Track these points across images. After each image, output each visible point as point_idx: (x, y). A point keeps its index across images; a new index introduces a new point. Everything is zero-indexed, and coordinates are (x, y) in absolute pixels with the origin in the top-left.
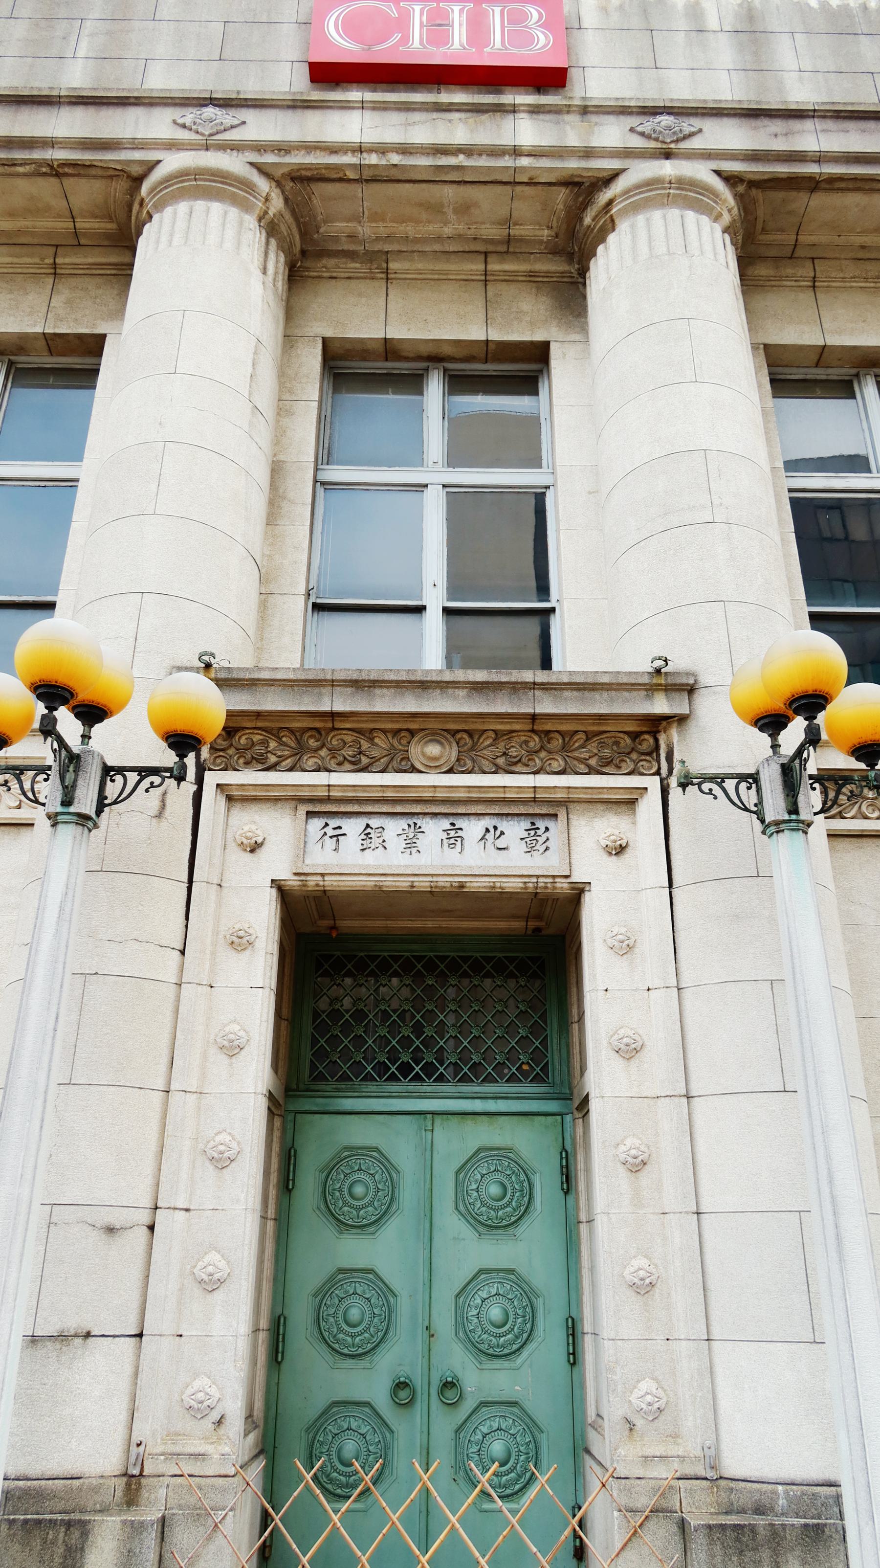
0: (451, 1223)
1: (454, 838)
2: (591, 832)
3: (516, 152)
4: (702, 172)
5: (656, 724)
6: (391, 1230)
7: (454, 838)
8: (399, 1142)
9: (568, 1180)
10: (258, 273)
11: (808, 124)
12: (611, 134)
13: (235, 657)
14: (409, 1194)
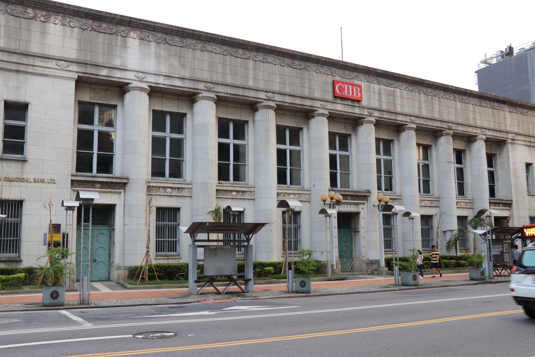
1: (351, 207)
2: (361, 206)
7: (351, 207)
9: (351, 238)
11: (385, 113)
12: (366, 112)
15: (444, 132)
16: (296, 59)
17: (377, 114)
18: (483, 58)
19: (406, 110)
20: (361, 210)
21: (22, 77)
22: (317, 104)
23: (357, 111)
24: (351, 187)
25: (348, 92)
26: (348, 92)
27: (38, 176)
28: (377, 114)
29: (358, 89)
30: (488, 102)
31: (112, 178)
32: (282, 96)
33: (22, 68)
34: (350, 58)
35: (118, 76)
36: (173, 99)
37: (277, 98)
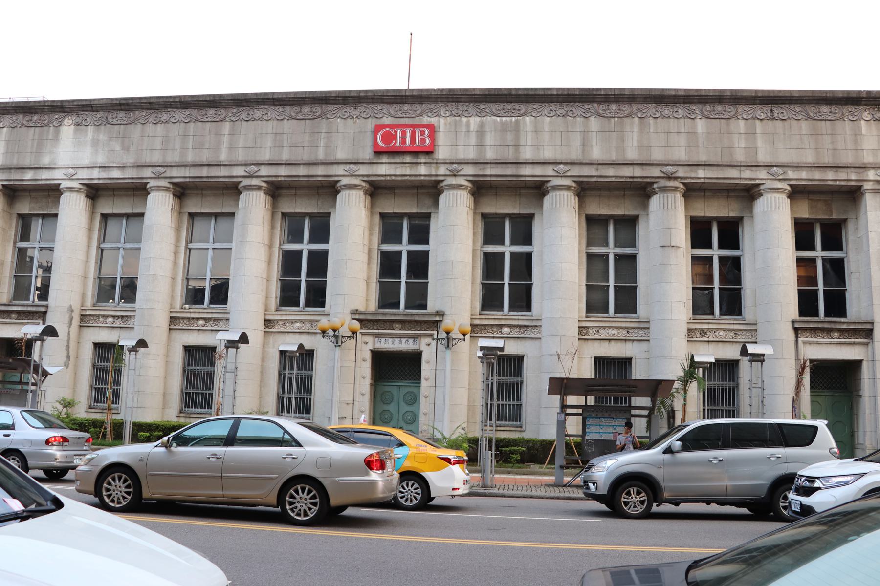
0: (402, 403)
1: (400, 342)
2: (425, 341)
3: (421, 176)
4: (462, 181)
5: (437, 322)
6: (392, 404)
7: (400, 342)
8: (394, 391)
10: (363, 208)
11: (489, 166)
12: (442, 170)
13: (361, 308)
14: (395, 399)
15: (655, 186)
16: (304, 104)
17: (469, 170)
20: (423, 348)
22: (339, 170)
23: (423, 170)
25: (403, 141)
26: (403, 139)
28: (469, 170)
29: (426, 131)
30: (798, 108)
31: (28, 306)
32: (290, 167)
34: (422, 82)
35: (44, 177)
36: (127, 196)
37: (264, 171)
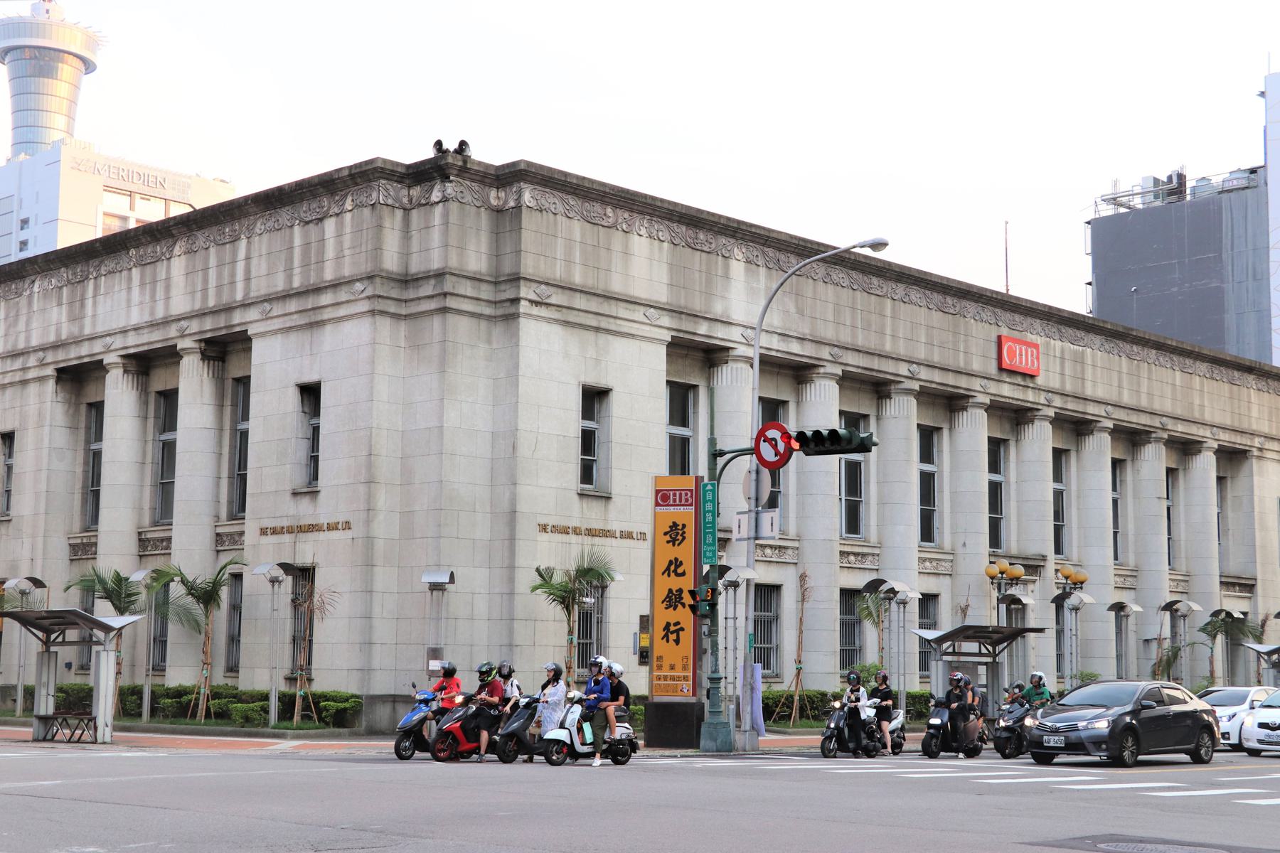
16: (948, 294)
18: (1108, 191)
19: (1100, 393)
21: (603, 337)
23: (1030, 396)
24: (1004, 544)
26: (1020, 358)
27: (627, 527)
28: (1058, 402)
33: (604, 323)
35: (721, 334)
